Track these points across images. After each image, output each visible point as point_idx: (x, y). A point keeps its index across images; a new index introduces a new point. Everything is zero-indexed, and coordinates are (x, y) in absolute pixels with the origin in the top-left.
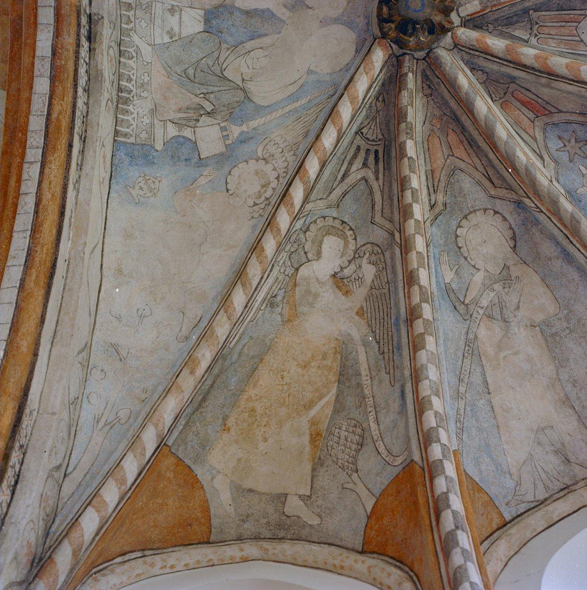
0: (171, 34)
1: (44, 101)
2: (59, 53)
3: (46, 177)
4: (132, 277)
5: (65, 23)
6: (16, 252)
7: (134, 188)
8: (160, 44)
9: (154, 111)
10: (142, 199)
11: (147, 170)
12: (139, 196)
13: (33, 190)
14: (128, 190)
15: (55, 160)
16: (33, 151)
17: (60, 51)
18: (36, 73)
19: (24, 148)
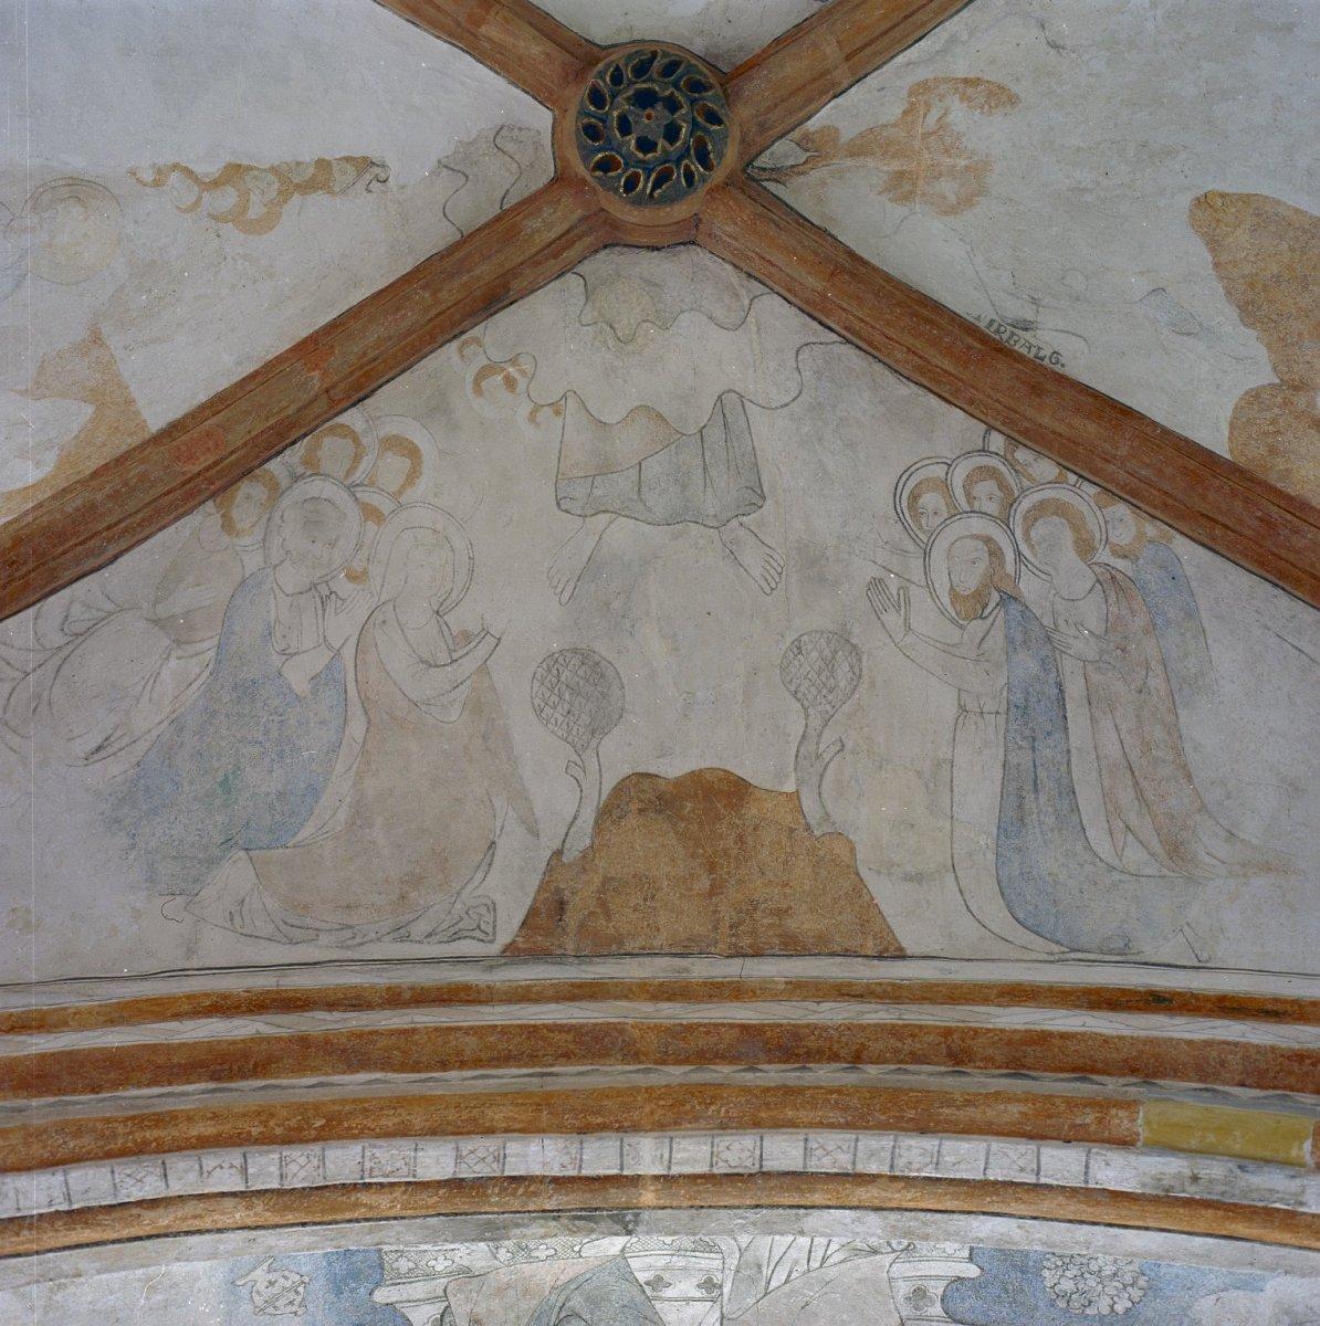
0: (658, 1282)
1: (396, 1174)
2: (516, 1189)
3: (212, 1205)
4: (46, 1313)
5: (589, 1195)
6: (11, 1194)
7: (269, 1272)
8: (629, 1266)
9: (466, 1273)
10: (244, 1292)
11: (319, 1285)
12: (250, 1284)
13: (176, 1188)
14: (261, 1263)
15: (256, 1215)
16: (274, 1169)
17: (520, 1191)
18: (467, 1145)
19: (287, 1141)
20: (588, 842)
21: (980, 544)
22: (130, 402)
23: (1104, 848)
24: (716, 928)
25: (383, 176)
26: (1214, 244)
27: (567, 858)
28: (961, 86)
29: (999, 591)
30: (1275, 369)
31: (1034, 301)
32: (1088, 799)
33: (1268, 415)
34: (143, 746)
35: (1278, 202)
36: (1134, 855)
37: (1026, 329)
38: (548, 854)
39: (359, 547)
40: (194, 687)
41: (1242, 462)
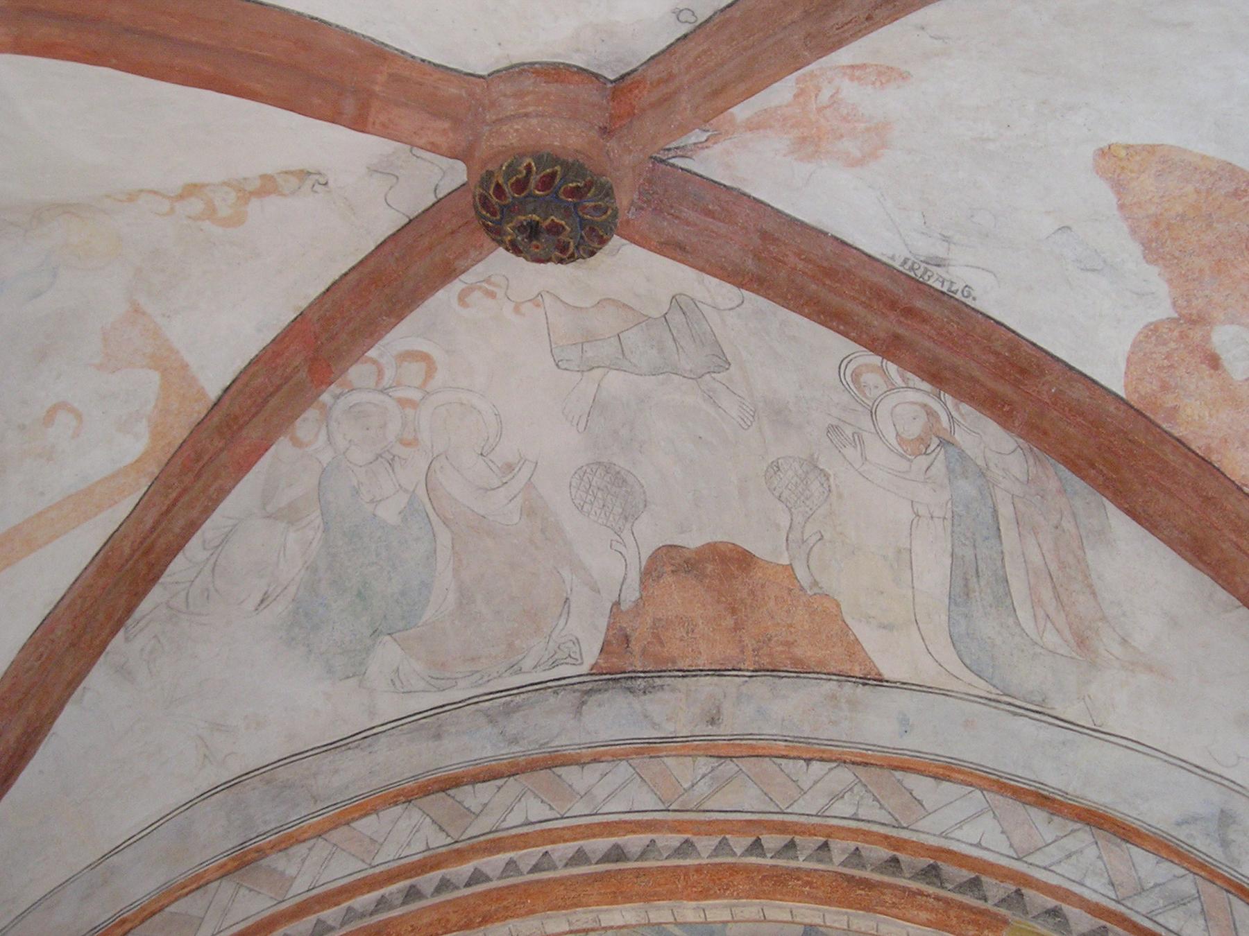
20: (637, 595)
21: (918, 408)
22: (185, 366)
23: (1029, 625)
24: (742, 652)
25: (322, 181)
26: (1119, 187)
27: (624, 607)
28: (848, 71)
29: (938, 437)
30: (1174, 304)
31: (946, 239)
32: (1018, 587)
33: (1164, 350)
34: (293, 589)
35: (1185, 151)
36: (1051, 638)
37: (938, 266)
38: (609, 605)
39: (404, 425)
40: (314, 544)
41: (1134, 400)
